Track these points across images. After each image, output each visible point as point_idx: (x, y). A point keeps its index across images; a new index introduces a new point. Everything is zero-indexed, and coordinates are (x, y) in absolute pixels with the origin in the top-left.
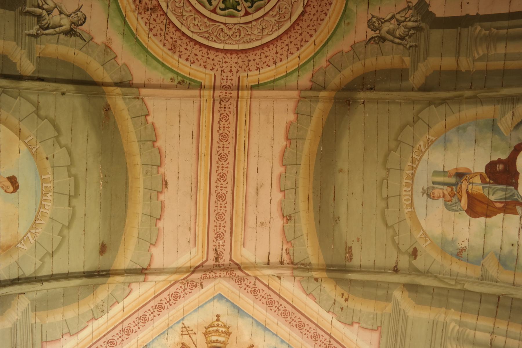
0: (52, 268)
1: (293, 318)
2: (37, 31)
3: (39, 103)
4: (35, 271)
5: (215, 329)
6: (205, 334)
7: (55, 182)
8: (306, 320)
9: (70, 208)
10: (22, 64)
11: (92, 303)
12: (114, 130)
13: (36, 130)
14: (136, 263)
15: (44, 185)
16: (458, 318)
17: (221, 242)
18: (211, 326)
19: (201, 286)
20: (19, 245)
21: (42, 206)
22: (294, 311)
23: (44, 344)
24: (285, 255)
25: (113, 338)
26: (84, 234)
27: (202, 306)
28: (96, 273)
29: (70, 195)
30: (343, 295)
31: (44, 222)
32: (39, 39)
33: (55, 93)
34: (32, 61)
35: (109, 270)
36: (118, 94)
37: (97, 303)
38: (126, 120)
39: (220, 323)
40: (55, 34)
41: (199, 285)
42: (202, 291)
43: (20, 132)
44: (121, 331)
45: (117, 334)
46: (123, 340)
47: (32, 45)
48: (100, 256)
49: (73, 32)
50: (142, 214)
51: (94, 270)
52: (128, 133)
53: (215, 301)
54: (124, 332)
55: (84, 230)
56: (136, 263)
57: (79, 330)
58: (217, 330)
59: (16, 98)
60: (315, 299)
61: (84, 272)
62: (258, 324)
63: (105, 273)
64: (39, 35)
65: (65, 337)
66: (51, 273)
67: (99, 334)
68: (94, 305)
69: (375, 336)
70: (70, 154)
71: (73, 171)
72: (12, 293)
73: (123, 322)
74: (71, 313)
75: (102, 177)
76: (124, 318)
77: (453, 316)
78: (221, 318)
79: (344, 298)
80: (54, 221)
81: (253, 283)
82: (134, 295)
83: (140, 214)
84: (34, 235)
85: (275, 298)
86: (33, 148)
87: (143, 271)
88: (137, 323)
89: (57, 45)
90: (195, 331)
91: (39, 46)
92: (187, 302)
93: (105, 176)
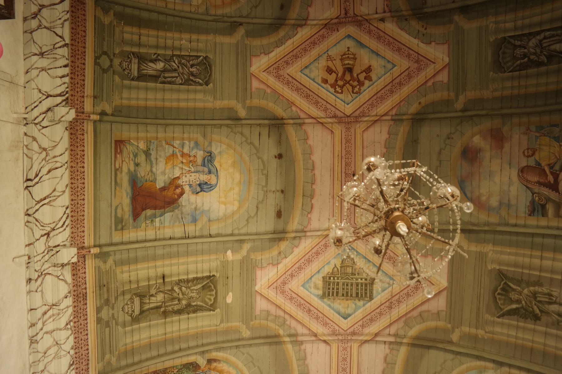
1: (394, 45)
5: (347, 56)
6: (341, 60)
8: (402, 46)
16: (494, 20)
17: (348, 4)
18: (344, 55)
19: (338, 31)
22: (394, 41)
24: (386, 8)
27: (338, 42)
30: (423, 26)
39: (350, 52)
41: (336, 30)
42: (339, 33)
53: (346, 39)
58: (348, 57)
60: (406, 32)
62: (373, 52)
65: (262, 55)
67: (280, 56)
69: (446, 46)
73: (293, 51)
74: (265, 41)
77: (492, 19)
78: (350, 49)
79: (424, 28)
81: (368, 27)
82: (299, 36)
85: (382, 34)
90: (335, 58)
92: (330, 40)
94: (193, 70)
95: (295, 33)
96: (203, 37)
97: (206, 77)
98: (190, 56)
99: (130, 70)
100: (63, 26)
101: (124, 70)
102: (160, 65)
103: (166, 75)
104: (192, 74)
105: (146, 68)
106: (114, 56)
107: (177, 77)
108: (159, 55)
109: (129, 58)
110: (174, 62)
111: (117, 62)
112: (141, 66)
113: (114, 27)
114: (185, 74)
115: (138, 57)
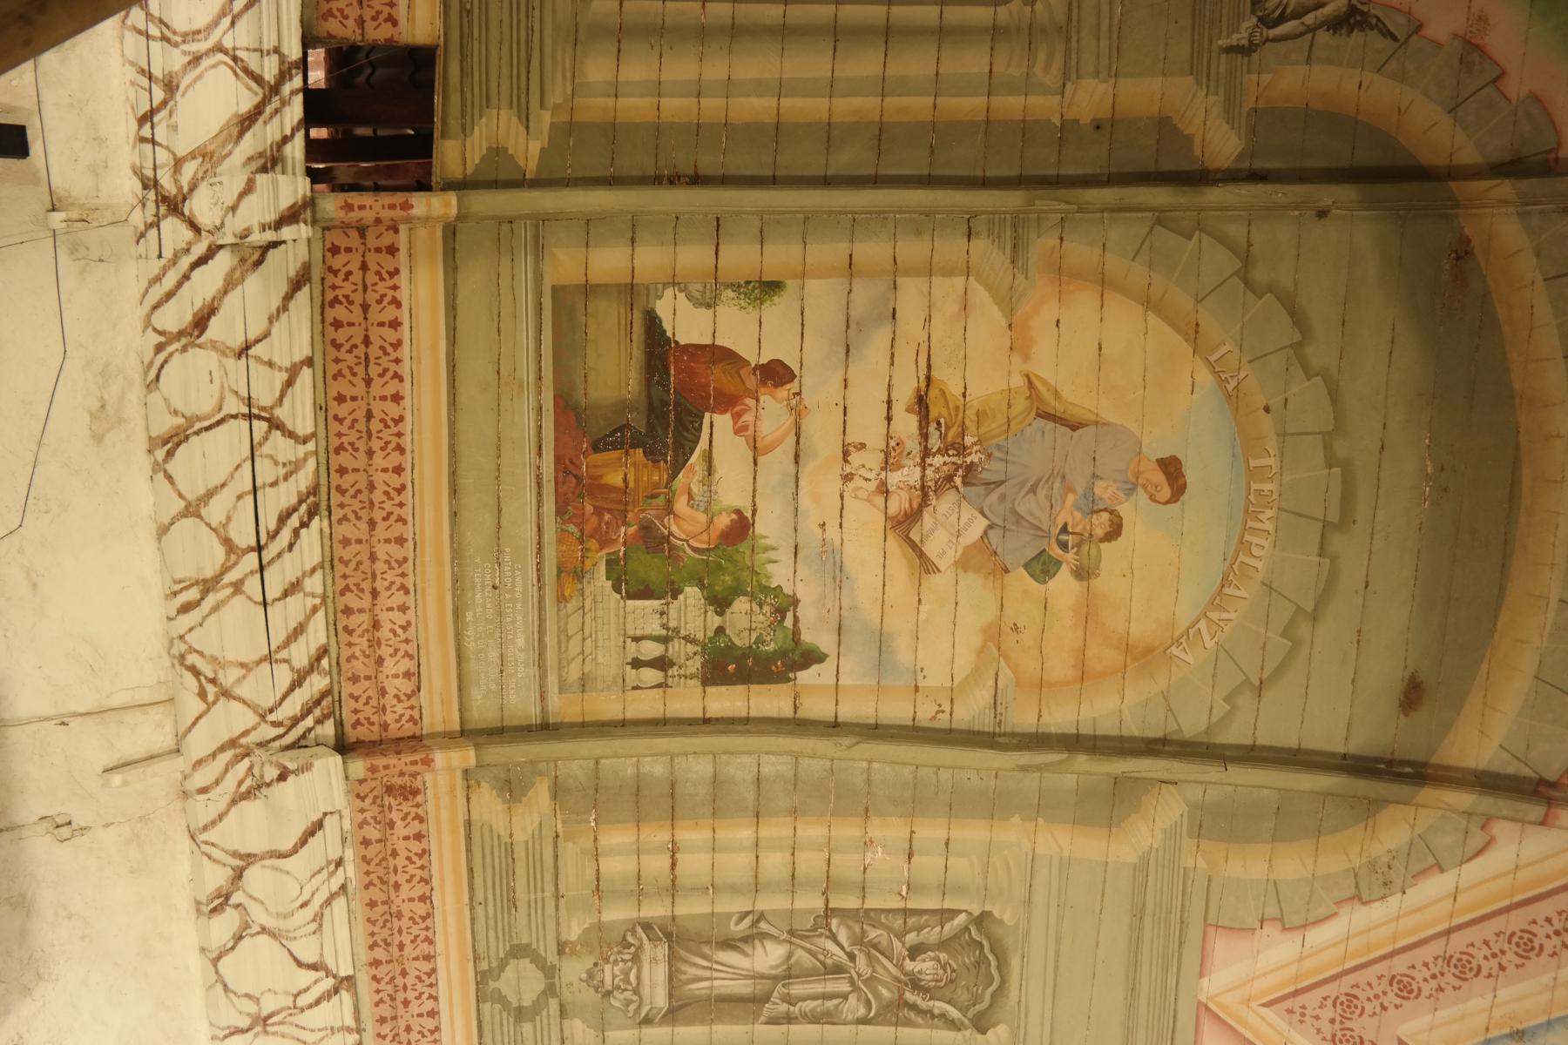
0: (1255, 728)
2: (1251, 35)
3: (1250, 245)
4: (1208, 728)
7: (1286, 478)
9: (1322, 560)
10: (1208, 137)
11: (1359, 849)
12: (1481, 321)
13: (1239, 325)
14: (1518, 759)
15: (1254, 486)
20: (1175, 650)
21: (1243, 546)
23: (1211, 931)
25: (1411, 972)
26: (1358, 642)
28: (1383, 766)
29: (1325, 521)
31: (1245, 592)
32: (1255, 56)
33: (1297, 213)
34: (1236, 126)
35: (1425, 765)
36: (1505, 202)
37: (1373, 856)
38: (1526, 287)
40: (1302, 34)
43: (1197, 332)
44: (1440, 960)
45: (1426, 965)
46: (1441, 989)
47: (1235, 77)
48: (1402, 717)
49: (1358, 18)
50: (1561, 601)
51: (1376, 754)
52: (1531, 330)
54: (1449, 966)
55: (1359, 631)
56: (1518, 759)
57: (1310, 920)
59: (1190, 238)
61: (1345, 756)
63: (1408, 770)
64: (1257, 45)
65: (1267, 929)
66: (1249, 742)
68: (1364, 860)
70: (1334, 396)
71: (1341, 448)
72: (1144, 775)
73: (1448, 932)
74: (1292, 865)
75: (1429, 470)
76: (1457, 921)
80: (1273, 593)
83: (1554, 602)
84: (1216, 628)
86: (1230, 379)
87: (1542, 789)
88: (1496, 949)
89: (1308, 67)
91: (1254, 77)
93: (1442, 469)
94: (924, 967)
95: (1478, 839)
96: (972, 833)
97: (976, 999)
98: (907, 912)
99: (636, 991)
100: (321, 925)
101: (608, 994)
102: (768, 957)
103: (797, 989)
104: (915, 984)
105: (707, 974)
106: (560, 952)
107: (845, 997)
108: (761, 916)
109: (630, 945)
110: (834, 938)
111: (573, 971)
112: (684, 967)
113: (556, 846)
114: (880, 982)
115: (669, 935)
